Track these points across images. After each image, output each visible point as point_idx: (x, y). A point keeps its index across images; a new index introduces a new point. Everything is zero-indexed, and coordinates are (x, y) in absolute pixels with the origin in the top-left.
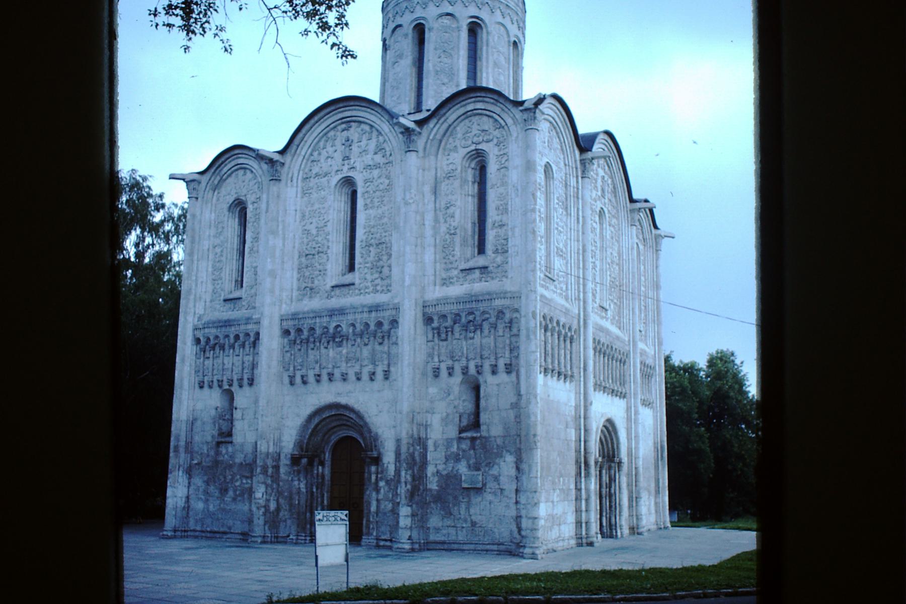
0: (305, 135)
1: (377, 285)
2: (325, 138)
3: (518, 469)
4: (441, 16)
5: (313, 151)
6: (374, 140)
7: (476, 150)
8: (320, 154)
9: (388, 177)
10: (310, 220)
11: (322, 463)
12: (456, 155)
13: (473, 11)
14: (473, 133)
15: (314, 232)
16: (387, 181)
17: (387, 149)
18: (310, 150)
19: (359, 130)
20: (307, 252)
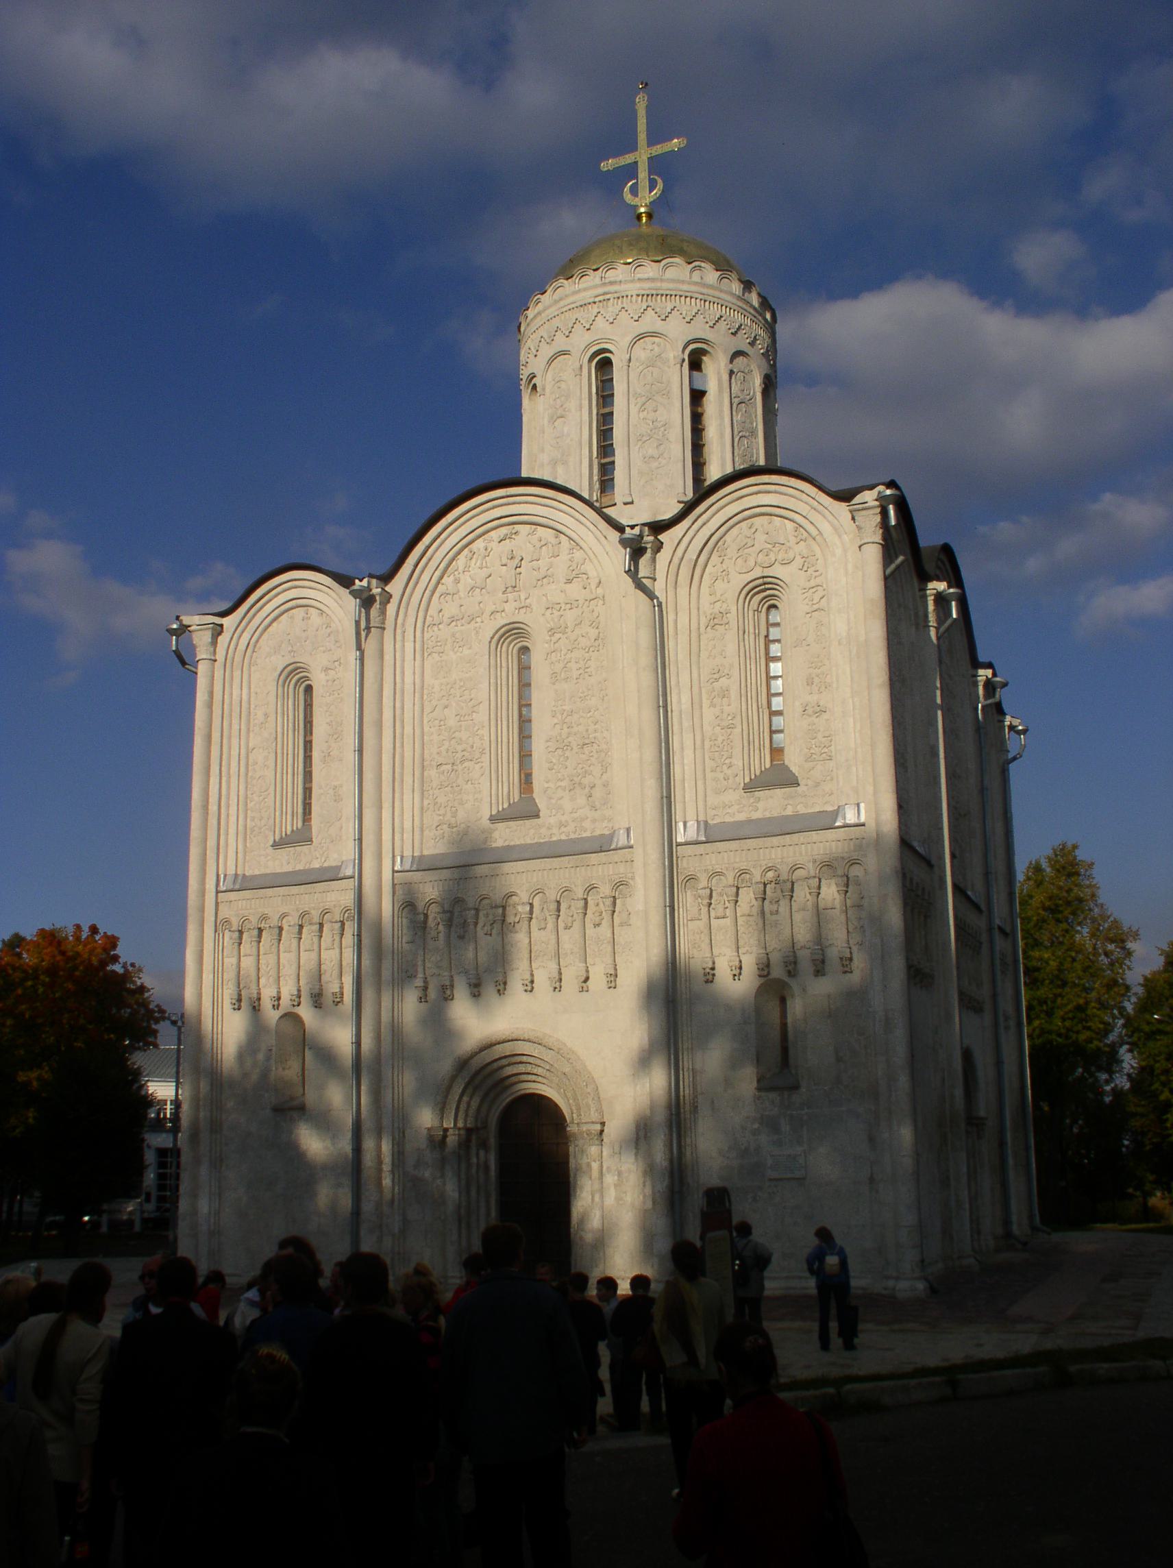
0: (428, 547)
1: (583, 819)
3: (871, 1139)
4: (641, 337)
5: (441, 577)
6: (564, 557)
8: (457, 581)
9: (595, 624)
10: (444, 701)
11: (484, 1145)
13: (700, 330)
14: (757, 548)
15: (452, 722)
16: (593, 633)
17: (592, 574)
18: (438, 573)
20: (441, 760)
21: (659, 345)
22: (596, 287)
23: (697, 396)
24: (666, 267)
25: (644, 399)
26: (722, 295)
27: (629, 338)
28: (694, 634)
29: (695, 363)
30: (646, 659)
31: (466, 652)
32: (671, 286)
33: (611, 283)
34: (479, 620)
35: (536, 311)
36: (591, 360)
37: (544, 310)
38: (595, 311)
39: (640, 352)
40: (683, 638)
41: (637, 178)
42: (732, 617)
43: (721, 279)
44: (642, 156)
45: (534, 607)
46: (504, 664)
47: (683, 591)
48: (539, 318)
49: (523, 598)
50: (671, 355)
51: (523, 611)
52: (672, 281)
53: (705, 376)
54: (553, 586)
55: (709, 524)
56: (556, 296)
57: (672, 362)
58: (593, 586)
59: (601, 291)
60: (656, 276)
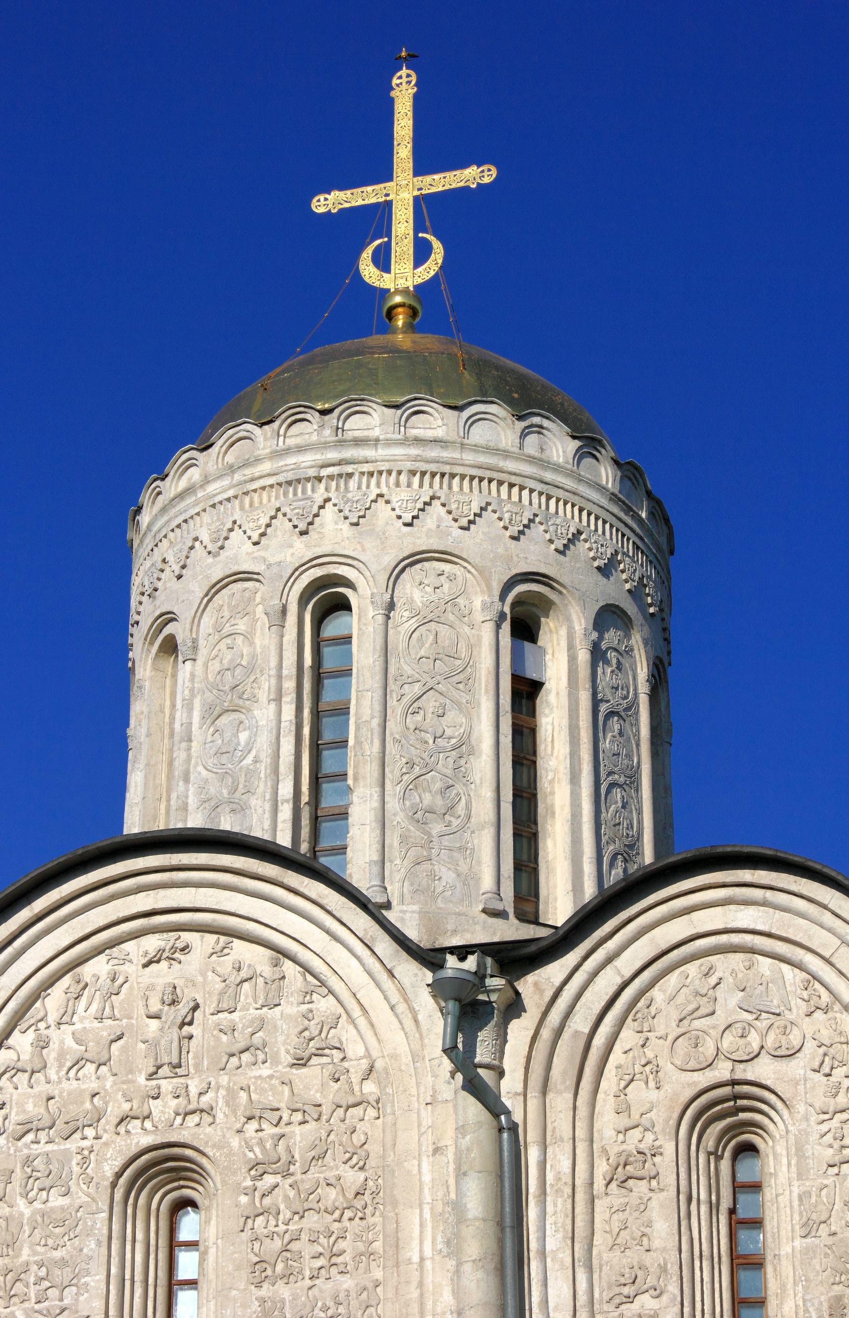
2: (67, 980)
4: (415, 559)
7: (734, 1083)
8: (42, 1044)
12: (653, 1095)
13: (534, 554)
14: (721, 1019)
16: (353, 1178)
17: (355, 1049)
19: (226, 965)
21: (451, 579)
22: (324, 446)
23: (526, 691)
24: (472, 421)
25: (417, 689)
26: (583, 489)
27: (390, 559)
28: (581, 1197)
29: (524, 627)
30: (476, 1244)
31: (56, 1201)
32: (482, 459)
33: (359, 442)
34: (90, 1132)
35: (183, 484)
36: (304, 599)
37: (206, 480)
38: (321, 493)
39: (414, 591)
40: (557, 1205)
41: (389, 235)
42: (665, 1163)
43: (580, 456)
44: (403, 190)
45: (220, 1116)
46: (140, 1236)
47: (559, 1102)
48: (190, 500)
49: (193, 1091)
50: (477, 603)
51: (196, 1118)
52: (488, 450)
53: (543, 651)
54: (265, 1071)
55: (618, 963)
56: (230, 458)
57: (478, 616)
58: (355, 1078)
59: (333, 455)
60: (452, 436)
